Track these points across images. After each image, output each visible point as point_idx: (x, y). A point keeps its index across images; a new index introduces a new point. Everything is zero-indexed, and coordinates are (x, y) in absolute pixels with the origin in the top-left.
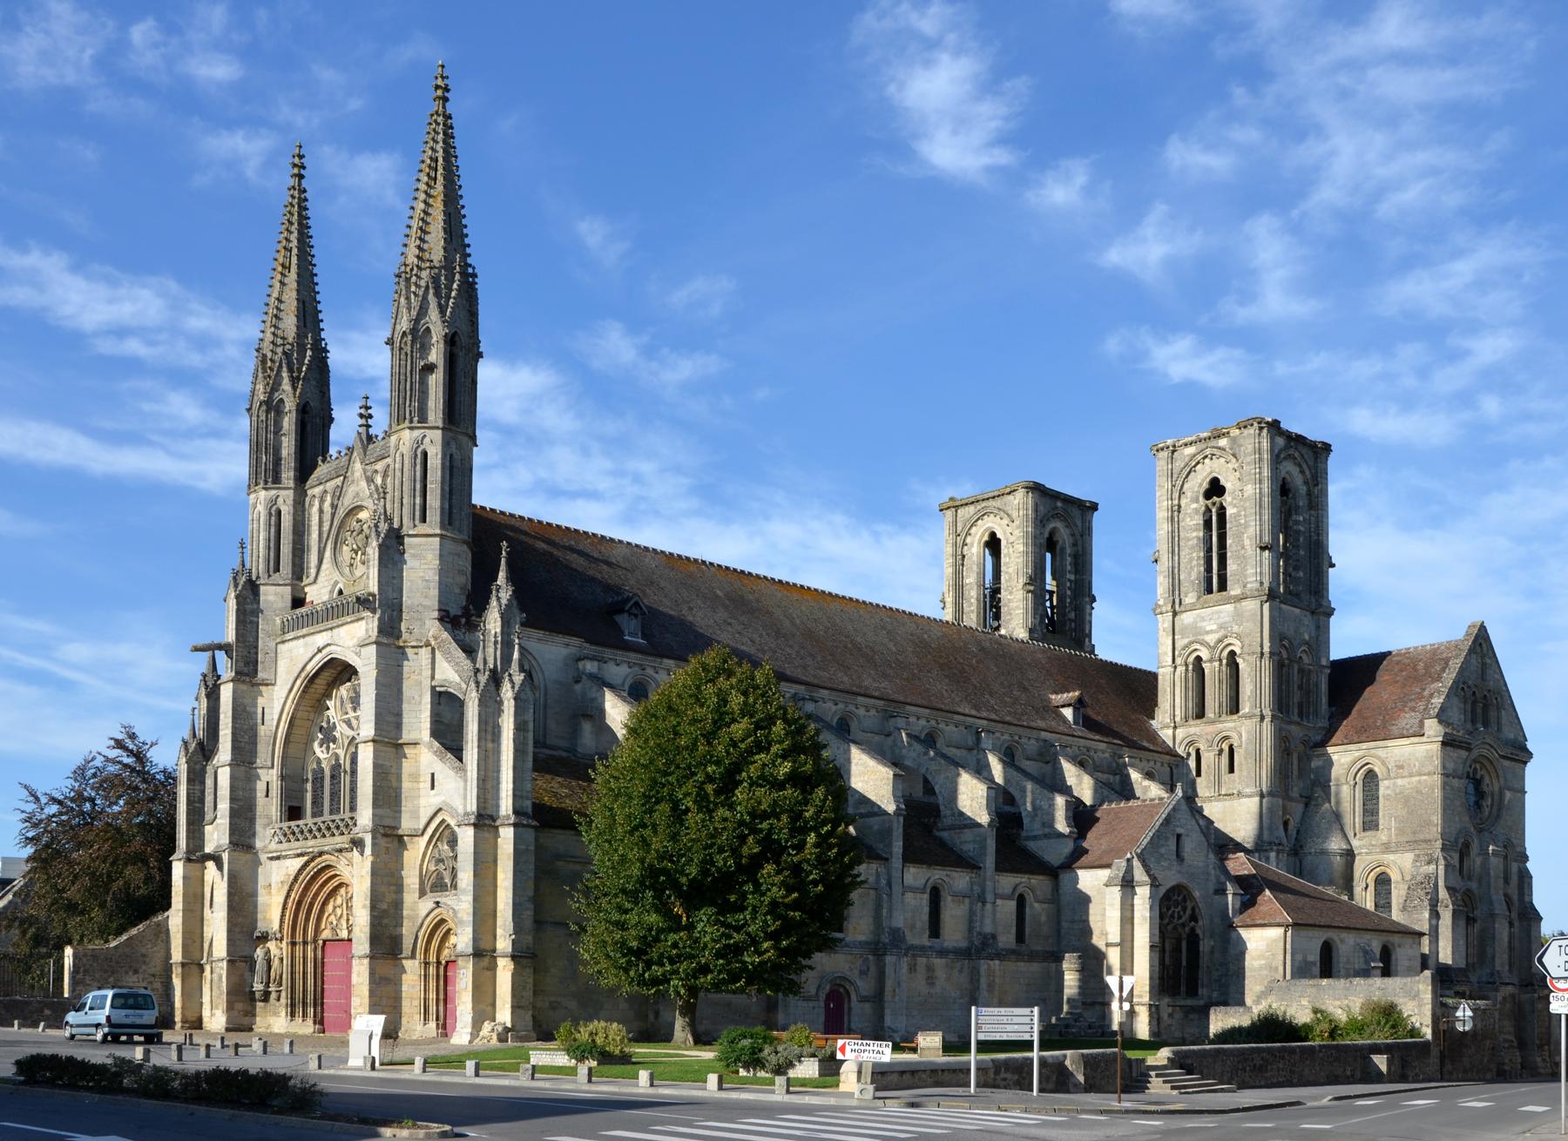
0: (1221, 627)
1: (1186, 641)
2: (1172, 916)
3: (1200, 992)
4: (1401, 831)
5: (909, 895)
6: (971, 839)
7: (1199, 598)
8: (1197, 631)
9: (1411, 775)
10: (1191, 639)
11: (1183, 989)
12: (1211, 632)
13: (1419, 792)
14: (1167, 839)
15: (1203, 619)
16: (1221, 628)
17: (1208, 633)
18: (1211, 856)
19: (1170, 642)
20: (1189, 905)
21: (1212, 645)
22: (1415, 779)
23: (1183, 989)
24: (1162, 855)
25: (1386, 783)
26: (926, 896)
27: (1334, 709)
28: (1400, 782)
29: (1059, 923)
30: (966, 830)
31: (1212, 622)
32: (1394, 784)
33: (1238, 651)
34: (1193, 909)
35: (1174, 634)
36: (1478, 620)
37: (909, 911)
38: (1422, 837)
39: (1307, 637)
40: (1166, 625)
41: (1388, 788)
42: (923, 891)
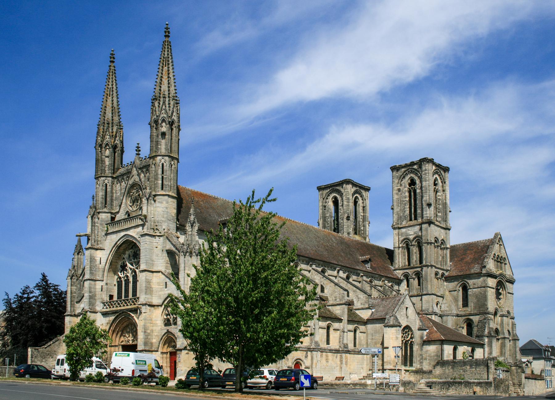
0: (415, 233)
1: (403, 238)
2: (405, 337)
3: (414, 365)
4: (475, 308)
5: (320, 329)
7: (407, 223)
10: (405, 237)
11: (408, 364)
13: (481, 293)
14: (403, 309)
17: (410, 235)
18: (417, 315)
19: (397, 238)
20: (410, 333)
23: (408, 364)
24: (402, 315)
25: (470, 290)
26: (326, 330)
27: (451, 263)
29: (367, 340)
34: (411, 335)
36: (497, 231)
37: (320, 335)
39: (443, 237)
42: (325, 328)
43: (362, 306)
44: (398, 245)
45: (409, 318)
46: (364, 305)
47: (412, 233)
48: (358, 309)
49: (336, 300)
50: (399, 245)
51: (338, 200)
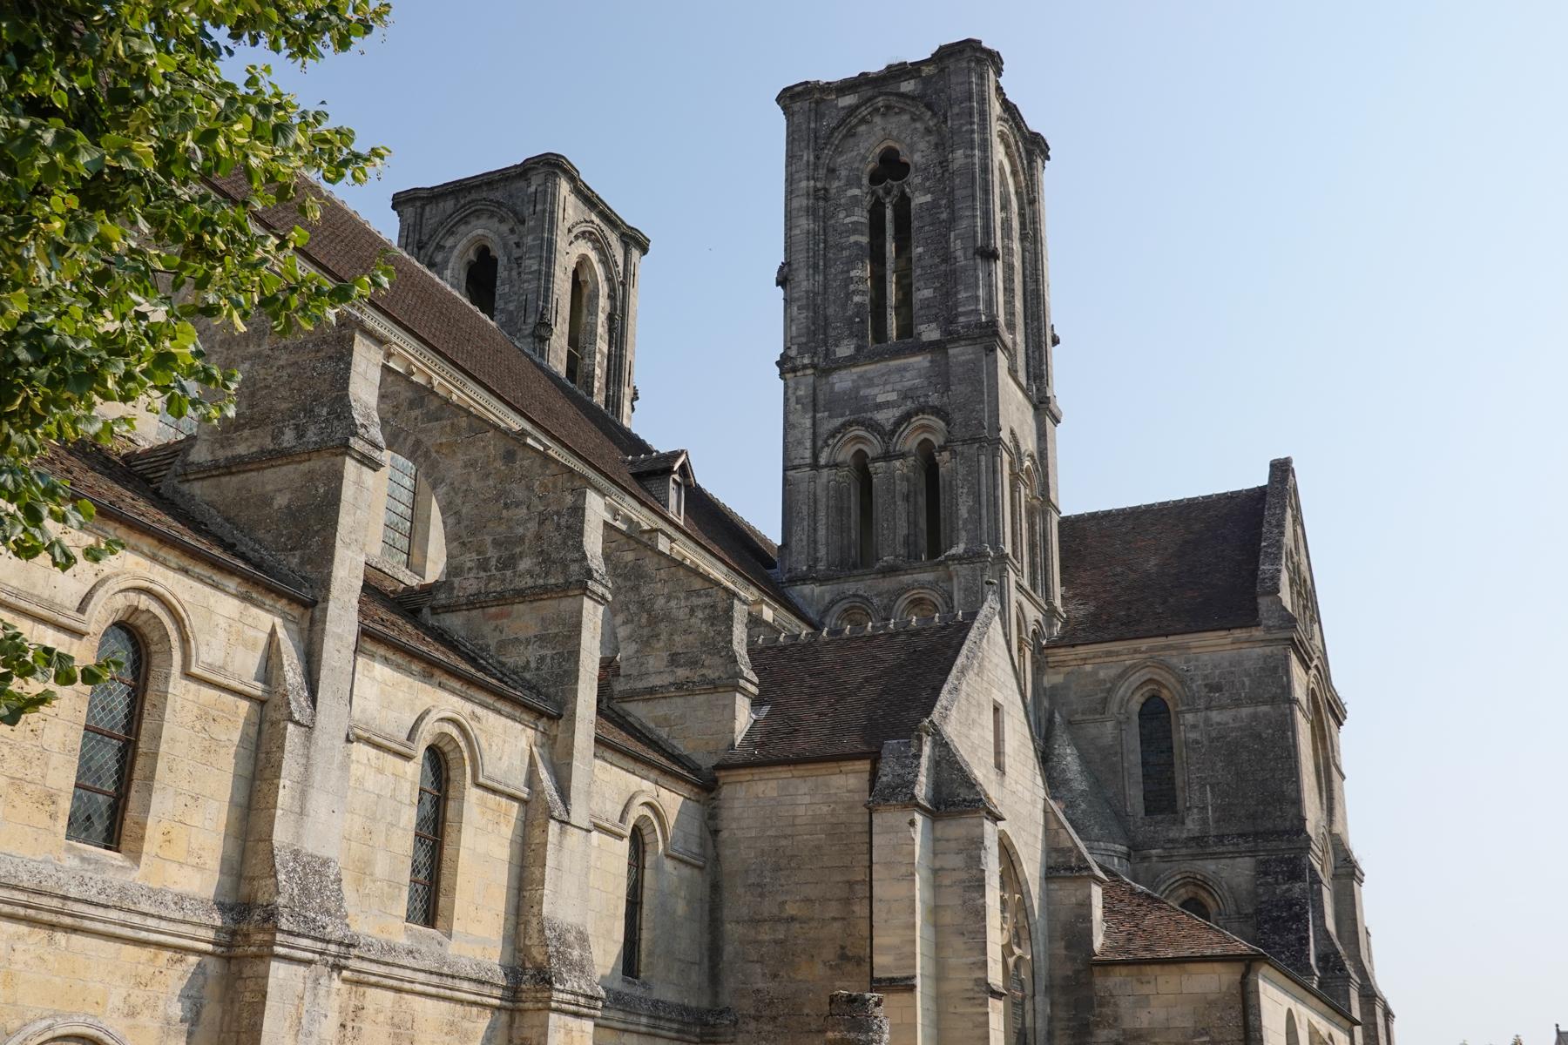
1: (838, 422)
6: (532, 632)
8: (858, 413)
9: (1237, 703)
12: (887, 405)
13: (1258, 737)
15: (870, 383)
16: (905, 397)
17: (880, 407)
19: (808, 423)
21: (888, 428)
22: (1245, 711)
25: (1189, 718)
28: (1215, 716)
30: (520, 608)
31: (889, 387)
32: (1207, 720)
33: (937, 440)
35: (815, 411)
38: (1269, 825)
40: (801, 393)
41: (1194, 727)
43: (682, 673)
44: (808, 454)
45: (1007, 780)
46: (693, 663)
47: (893, 396)
48: (651, 693)
49: (509, 563)
50: (815, 456)
51: (495, 261)
